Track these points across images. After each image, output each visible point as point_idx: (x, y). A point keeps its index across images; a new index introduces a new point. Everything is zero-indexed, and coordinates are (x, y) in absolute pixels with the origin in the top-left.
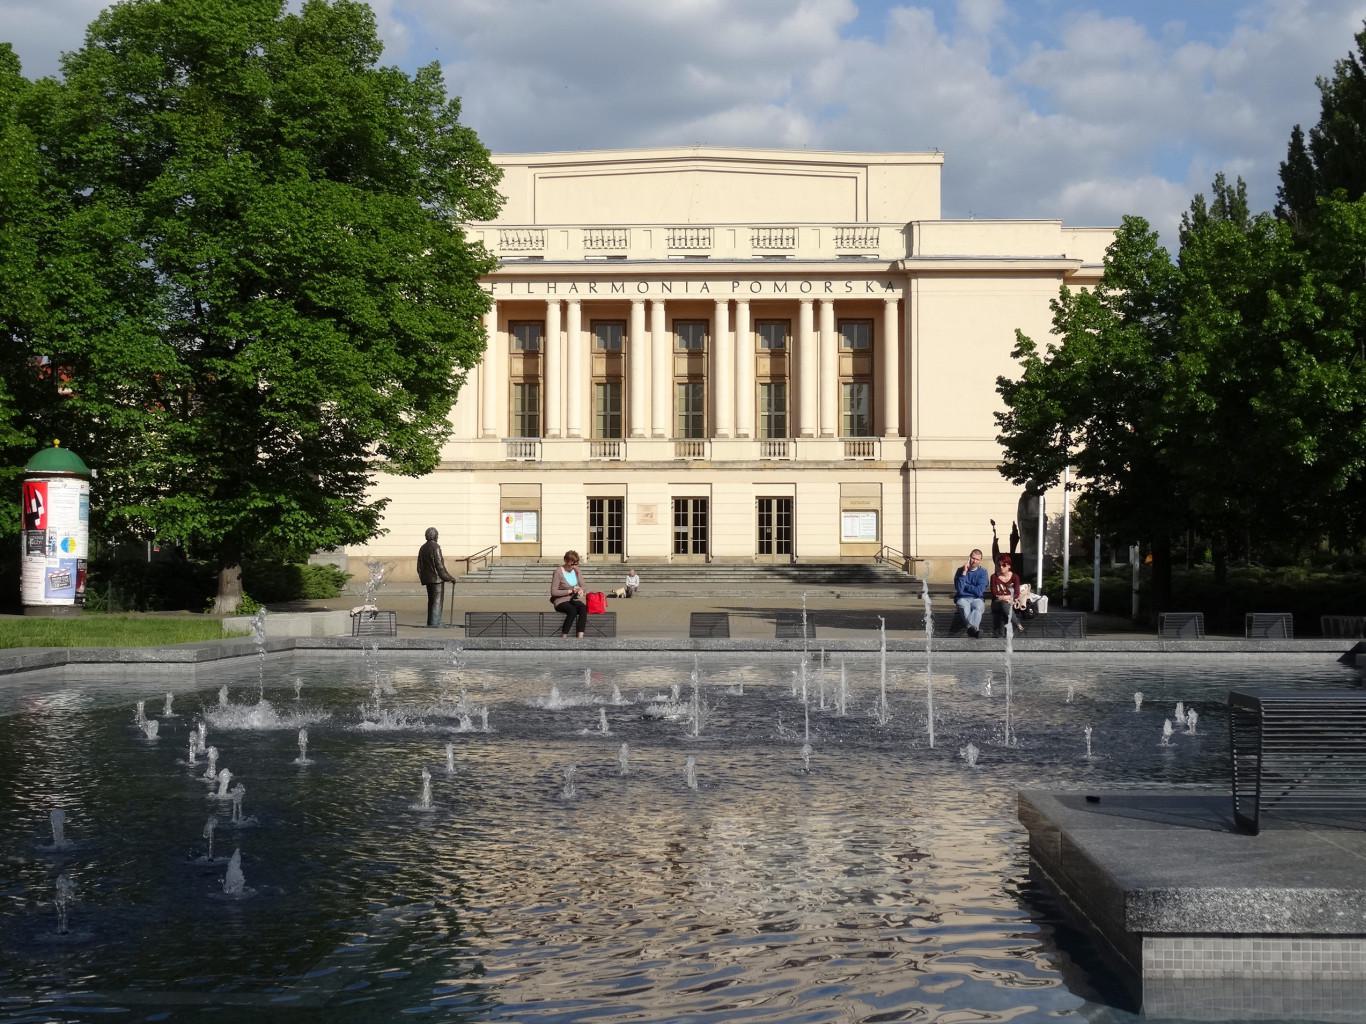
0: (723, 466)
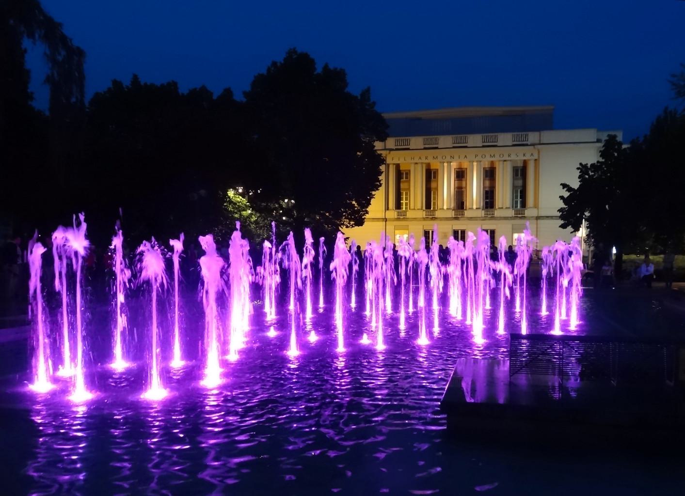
0: (471, 219)
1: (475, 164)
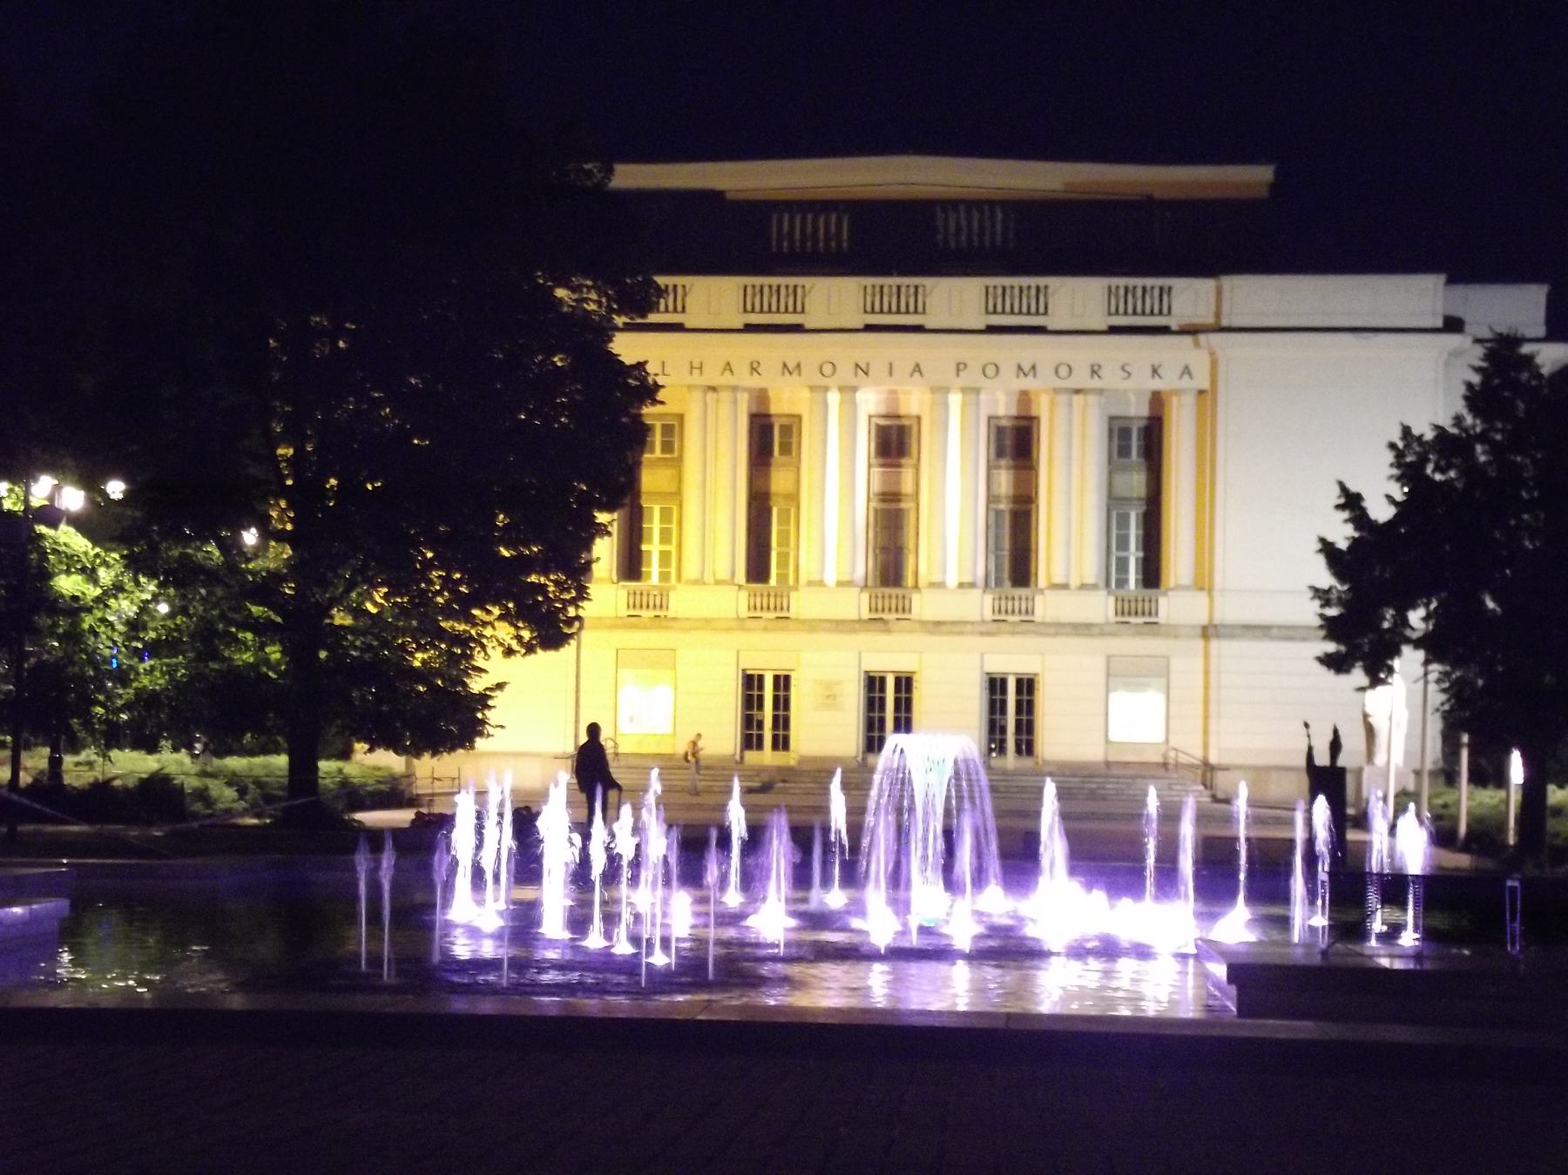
0: (937, 626)
1: (955, 399)
